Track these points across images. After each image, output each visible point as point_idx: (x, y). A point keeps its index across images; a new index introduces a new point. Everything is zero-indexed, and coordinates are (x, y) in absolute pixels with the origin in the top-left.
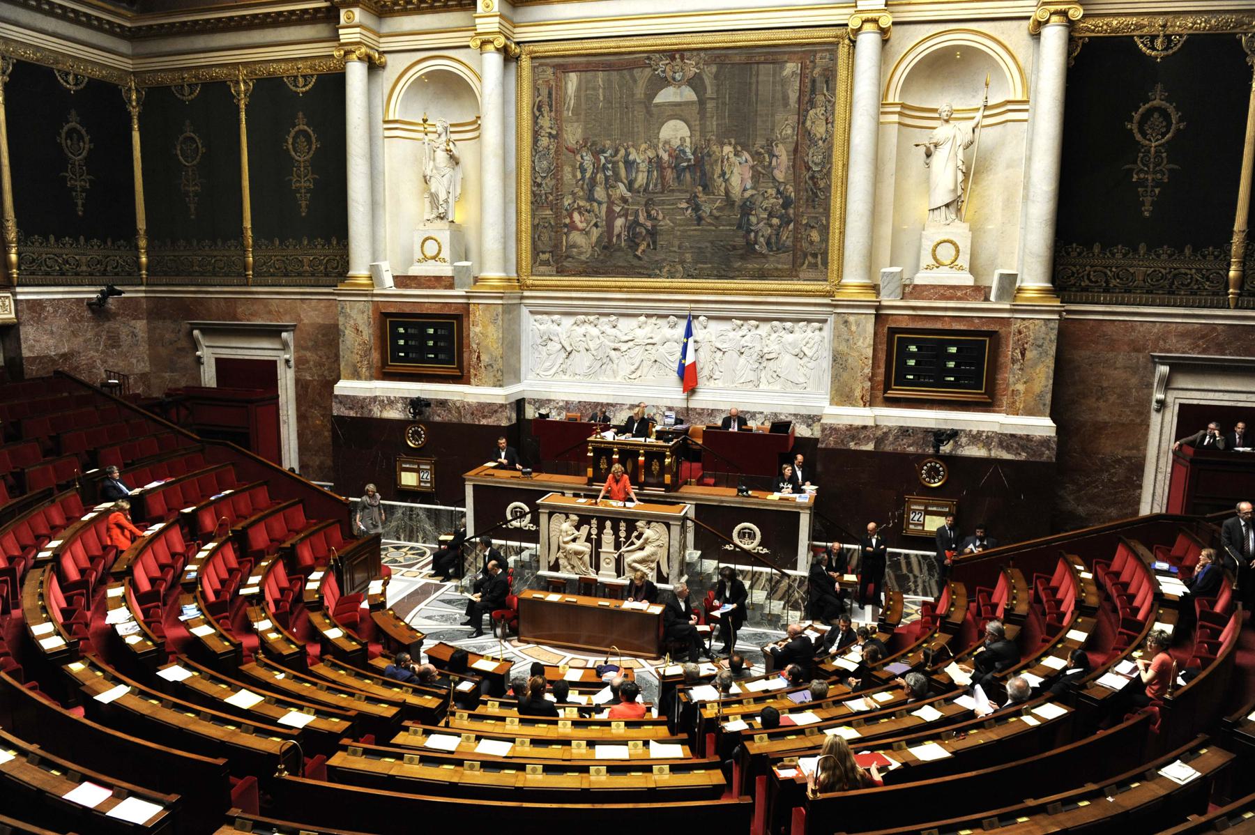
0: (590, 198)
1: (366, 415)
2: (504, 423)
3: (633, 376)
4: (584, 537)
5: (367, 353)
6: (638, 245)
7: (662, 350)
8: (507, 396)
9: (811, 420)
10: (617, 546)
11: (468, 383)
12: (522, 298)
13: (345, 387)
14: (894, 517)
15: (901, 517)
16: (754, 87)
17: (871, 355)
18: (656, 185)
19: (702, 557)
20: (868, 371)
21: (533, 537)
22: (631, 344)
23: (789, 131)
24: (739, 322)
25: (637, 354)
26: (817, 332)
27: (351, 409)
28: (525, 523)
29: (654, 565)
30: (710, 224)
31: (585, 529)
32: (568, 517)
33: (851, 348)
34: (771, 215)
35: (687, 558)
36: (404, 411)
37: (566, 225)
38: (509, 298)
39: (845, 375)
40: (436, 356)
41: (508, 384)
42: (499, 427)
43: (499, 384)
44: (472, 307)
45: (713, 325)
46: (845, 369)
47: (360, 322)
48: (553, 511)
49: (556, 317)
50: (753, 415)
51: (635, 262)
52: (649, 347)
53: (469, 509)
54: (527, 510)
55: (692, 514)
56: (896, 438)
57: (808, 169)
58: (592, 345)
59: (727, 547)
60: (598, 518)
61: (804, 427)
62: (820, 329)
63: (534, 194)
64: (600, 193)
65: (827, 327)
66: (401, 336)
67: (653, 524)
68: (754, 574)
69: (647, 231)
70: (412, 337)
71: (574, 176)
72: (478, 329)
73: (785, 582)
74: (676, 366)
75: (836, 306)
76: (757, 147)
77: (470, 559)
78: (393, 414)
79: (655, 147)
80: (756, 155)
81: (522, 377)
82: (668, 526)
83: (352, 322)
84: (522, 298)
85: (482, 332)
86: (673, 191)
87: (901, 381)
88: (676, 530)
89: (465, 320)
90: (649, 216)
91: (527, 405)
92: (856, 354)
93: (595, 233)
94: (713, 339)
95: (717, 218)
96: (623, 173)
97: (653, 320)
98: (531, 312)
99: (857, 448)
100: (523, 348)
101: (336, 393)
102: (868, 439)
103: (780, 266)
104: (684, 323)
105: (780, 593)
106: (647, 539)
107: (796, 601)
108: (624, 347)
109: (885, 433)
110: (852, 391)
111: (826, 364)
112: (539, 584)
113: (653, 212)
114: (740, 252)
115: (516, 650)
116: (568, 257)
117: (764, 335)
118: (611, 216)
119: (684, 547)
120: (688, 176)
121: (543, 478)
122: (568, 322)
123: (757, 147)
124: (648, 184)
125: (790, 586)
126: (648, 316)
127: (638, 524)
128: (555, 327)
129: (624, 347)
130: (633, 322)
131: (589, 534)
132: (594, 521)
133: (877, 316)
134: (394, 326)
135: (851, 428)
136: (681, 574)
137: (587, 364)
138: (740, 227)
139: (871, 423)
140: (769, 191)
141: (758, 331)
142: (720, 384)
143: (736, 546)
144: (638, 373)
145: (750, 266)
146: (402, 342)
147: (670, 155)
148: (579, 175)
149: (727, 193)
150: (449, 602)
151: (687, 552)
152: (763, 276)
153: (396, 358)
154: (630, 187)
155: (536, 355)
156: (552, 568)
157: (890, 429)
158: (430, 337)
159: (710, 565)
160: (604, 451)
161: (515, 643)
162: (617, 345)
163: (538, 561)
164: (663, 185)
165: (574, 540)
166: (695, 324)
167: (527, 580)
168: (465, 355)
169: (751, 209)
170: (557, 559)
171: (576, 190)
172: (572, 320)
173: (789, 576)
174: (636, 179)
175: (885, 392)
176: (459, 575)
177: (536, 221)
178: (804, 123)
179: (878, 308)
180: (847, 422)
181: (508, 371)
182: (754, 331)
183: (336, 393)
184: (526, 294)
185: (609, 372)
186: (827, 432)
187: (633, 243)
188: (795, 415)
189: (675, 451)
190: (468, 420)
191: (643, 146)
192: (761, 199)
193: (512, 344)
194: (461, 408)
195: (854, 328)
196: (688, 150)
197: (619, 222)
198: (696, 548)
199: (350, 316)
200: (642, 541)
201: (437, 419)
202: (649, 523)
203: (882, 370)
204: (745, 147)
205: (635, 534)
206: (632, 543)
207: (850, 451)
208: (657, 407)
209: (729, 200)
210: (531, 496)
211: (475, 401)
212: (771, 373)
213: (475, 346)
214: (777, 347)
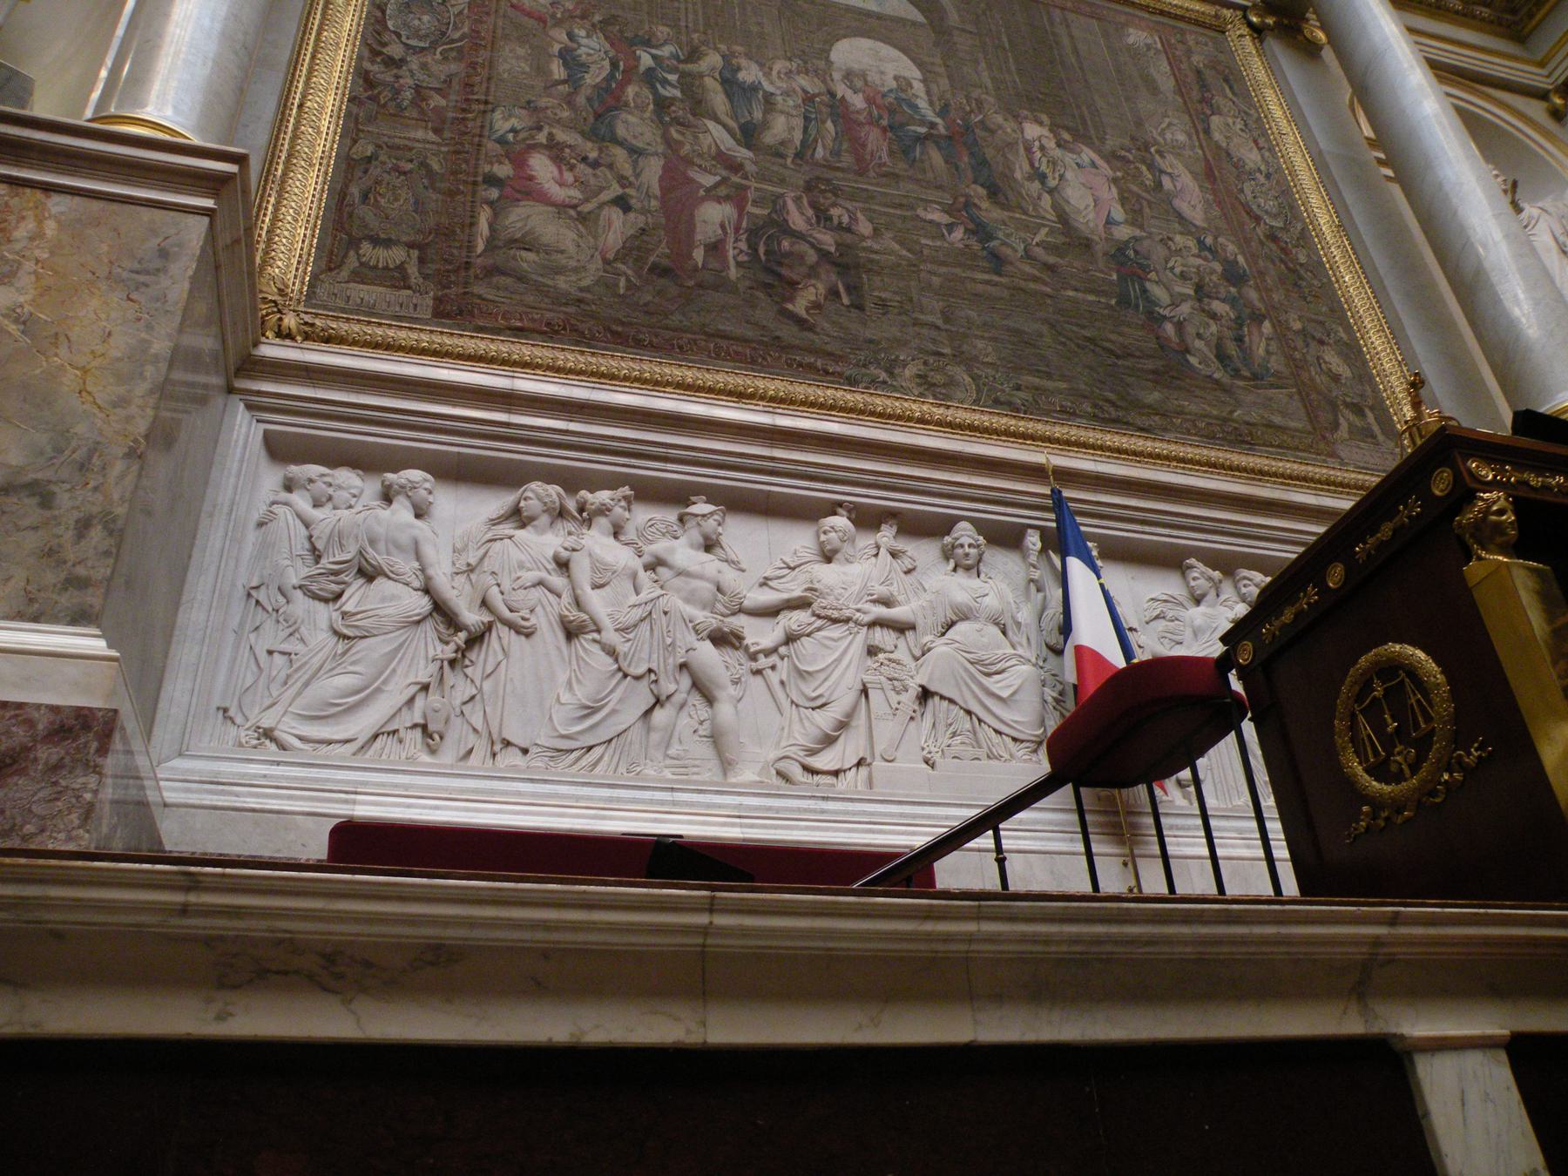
0: (600, 127)
3: (823, 761)
6: (793, 284)
16: (1066, 41)
18: (836, 153)
23: (1182, 137)
25: (836, 659)
30: (1035, 279)
34: (1202, 292)
37: (492, 180)
51: (788, 332)
52: (882, 637)
57: (1258, 219)
63: (363, 78)
64: (635, 125)
69: (824, 255)
71: (541, 70)
76: (1112, 142)
79: (824, 75)
80: (1112, 157)
86: (895, 176)
90: (822, 217)
93: (616, 228)
95: (1051, 268)
96: (718, 100)
100: (200, 586)
103: (1277, 420)
113: (835, 212)
114: (1149, 365)
116: (492, 271)
118: (678, 196)
120: (936, 157)
123: (1112, 142)
124: (807, 145)
129: (761, 634)
130: (797, 540)
137: (582, 694)
138: (1124, 301)
140: (1178, 238)
145: (1192, 407)
147: (870, 101)
148: (558, 70)
149: (1063, 218)
152: (1242, 438)
154: (748, 134)
164: (859, 159)
169: (1146, 269)
171: (544, 102)
174: (765, 125)
177: (365, 148)
178: (1207, 131)
184: (272, 350)
187: (773, 275)
191: (779, 65)
192: (1160, 251)
196: (922, 104)
197: (713, 216)
204: (1081, 136)
209: (1073, 240)
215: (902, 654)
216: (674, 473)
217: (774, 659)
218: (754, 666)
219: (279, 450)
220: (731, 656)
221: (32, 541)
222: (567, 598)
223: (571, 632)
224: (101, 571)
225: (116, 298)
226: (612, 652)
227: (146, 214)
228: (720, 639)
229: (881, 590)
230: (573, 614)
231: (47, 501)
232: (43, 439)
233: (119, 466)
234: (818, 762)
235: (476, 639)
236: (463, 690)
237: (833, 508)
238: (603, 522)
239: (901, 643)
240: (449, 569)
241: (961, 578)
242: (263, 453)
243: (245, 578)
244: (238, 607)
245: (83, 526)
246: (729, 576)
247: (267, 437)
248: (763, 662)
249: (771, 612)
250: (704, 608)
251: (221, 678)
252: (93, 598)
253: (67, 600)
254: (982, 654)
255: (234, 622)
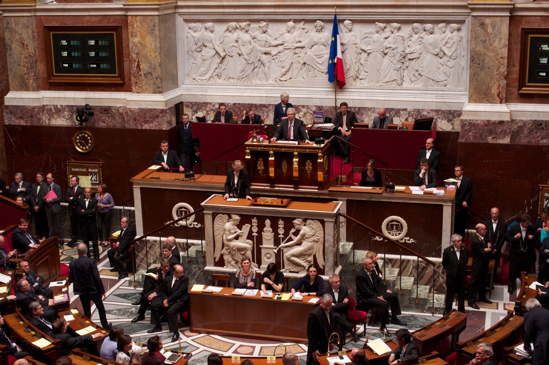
1: (35, 123)
2: (165, 127)
3: (282, 79)
4: (246, 235)
5: (33, 66)
7: (310, 52)
8: (167, 102)
9: (452, 115)
10: (277, 242)
11: (129, 90)
12: (177, 7)
13: (15, 97)
14: (529, 204)
15: (536, 203)
17: (506, 55)
19: (354, 248)
20: (503, 69)
21: (199, 234)
22: (281, 48)
24: (382, 25)
25: (287, 57)
26: (456, 33)
27: (21, 118)
28: (191, 222)
29: (311, 258)
31: (246, 228)
32: (230, 217)
33: (487, 49)
35: (341, 250)
36: (71, 118)
38: (165, 9)
39: (482, 74)
40: (98, 66)
41: (167, 91)
42: (161, 131)
43: (159, 90)
44: (130, 19)
45: (359, 29)
46: (482, 68)
47: (25, 36)
48: (216, 212)
49: (209, 24)
50: (397, 112)
53: (137, 208)
54: (192, 210)
55: (344, 211)
56: (531, 131)
58: (244, 50)
59: (377, 238)
60: (258, 217)
61: (445, 122)
62: (459, 30)
65: (465, 28)
66: (64, 48)
67: (309, 221)
68: (402, 261)
70: (75, 48)
72: (136, 40)
73: (431, 269)
74: (325, 68)
75: (473, 10)
77: (141, 255)
78: (60, 122)
81: (180, 82)
82: (323, 223)
83: (17, 37)
84: (177, 7)
85: (141, 42)
87: (535, 79)
88: (330, 226)
89: (124, 31)
91: (185, 108)
92: (491, 54)
94: (358, 41)
97: (301, 25)
98: (185, 21)
99: (494, 142)
101: (6, 103)
102: (504, 134)
104: (330, 27)
105: (426, 278)
106: (304, 235)
107: (441, 285)
108: (274, 51)
109: (521, 128)
110: (489, 88)
111: (465, 62)
112: (206, 278)
115: (189, 340)
117: (406, 36)
119: (337, 240)
121: (205, 180)
122: (220, 28)
125: (435, 272)
126: (295, 21)
127: (296, 221)
128: (208, 34)
129: (274, 51)
130: (283, 27)
131: (251, 232)
132: (254, 220)
133: (512, 18)
134: (57, 39)
135: (488, 123)
136: (336, 265)
137: (240, 68)
139: (507, 118)
141: (400, 34)
142: (365, 83)
143: (385, 238)
144: (289, 75)
146: (65, 54)
150: (125, 296)
151: (341, 244)
153: (60, 69)
155: (192, 60)
156: (216, 264)
157: (525, 123)
158: (92, 48)
159: (362, 255)
160: (260, 154)
161: (188, 333)
162: (267, 50)
163: (204, 257)
165: (237, 238)
166: (341, 26)
167: (194, 275)
168: (126, 64)
170: (222, 256)
172: (223, 27)
173: (433, 264)
175: (520, 89)
176: (131, 269)
179: (513, 10)
180: (485, 118)
181: (166, 78)
182: (397, 34)
183: (6, 103)
185: (261, 75)
186: (467, 128)
188: (437, 111)
189: (326, 152)
190: (131, 125)
193: (169, 52)
194: (123, 114)
195: (490, 30)
198: (348, 240)
199: (15, 32)
200: (299, 237)
201: (102, 125)
202: (305, 220)
203: (517, 69)
205: (293, 230)
206: (291, 239)
207: (488, 144)
208: (308, 107)
210: (196, 197)
211: (137, 107)
212: (413, 72)
213: (134, 56)
214: (418, 47)
215: (302, 54)
216: (256, 17)
217: (277, 56)
218: (273, 58)
219: (186, 21)
220: (268, 56)
221: (152, 81)
222: (238, 48)
223: (240, 55)
224: (160, 86)
225: (150, 36)
226: (246, 60)
227: (150, 17)
228: (265, 54)
229: (298, 39)
230: (239, 52)
231: (152, 75)
232: (148, 65)
233: (158, 68)
234: (282, 79)
235: (223, 58)
236: (223, 68)
237: (290, 20)
238: (243, 30)
239: (302, 51)
240: (218, 44)
241: (317, 34)
242: (184, 22)
243: (186, 49)
244: (186, 55)
245: (157, 78)
246: (269, 39)
247: (184, 19)
248: (275, 57)
249: (277, 46)
250: (263, 47)
251: (186, 68)
252: (160, 89)
253: (158, 90)
254: (318, 53)
255: (186, 58)
